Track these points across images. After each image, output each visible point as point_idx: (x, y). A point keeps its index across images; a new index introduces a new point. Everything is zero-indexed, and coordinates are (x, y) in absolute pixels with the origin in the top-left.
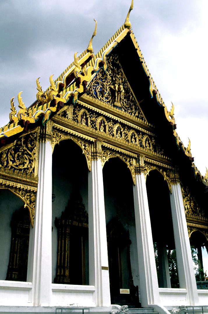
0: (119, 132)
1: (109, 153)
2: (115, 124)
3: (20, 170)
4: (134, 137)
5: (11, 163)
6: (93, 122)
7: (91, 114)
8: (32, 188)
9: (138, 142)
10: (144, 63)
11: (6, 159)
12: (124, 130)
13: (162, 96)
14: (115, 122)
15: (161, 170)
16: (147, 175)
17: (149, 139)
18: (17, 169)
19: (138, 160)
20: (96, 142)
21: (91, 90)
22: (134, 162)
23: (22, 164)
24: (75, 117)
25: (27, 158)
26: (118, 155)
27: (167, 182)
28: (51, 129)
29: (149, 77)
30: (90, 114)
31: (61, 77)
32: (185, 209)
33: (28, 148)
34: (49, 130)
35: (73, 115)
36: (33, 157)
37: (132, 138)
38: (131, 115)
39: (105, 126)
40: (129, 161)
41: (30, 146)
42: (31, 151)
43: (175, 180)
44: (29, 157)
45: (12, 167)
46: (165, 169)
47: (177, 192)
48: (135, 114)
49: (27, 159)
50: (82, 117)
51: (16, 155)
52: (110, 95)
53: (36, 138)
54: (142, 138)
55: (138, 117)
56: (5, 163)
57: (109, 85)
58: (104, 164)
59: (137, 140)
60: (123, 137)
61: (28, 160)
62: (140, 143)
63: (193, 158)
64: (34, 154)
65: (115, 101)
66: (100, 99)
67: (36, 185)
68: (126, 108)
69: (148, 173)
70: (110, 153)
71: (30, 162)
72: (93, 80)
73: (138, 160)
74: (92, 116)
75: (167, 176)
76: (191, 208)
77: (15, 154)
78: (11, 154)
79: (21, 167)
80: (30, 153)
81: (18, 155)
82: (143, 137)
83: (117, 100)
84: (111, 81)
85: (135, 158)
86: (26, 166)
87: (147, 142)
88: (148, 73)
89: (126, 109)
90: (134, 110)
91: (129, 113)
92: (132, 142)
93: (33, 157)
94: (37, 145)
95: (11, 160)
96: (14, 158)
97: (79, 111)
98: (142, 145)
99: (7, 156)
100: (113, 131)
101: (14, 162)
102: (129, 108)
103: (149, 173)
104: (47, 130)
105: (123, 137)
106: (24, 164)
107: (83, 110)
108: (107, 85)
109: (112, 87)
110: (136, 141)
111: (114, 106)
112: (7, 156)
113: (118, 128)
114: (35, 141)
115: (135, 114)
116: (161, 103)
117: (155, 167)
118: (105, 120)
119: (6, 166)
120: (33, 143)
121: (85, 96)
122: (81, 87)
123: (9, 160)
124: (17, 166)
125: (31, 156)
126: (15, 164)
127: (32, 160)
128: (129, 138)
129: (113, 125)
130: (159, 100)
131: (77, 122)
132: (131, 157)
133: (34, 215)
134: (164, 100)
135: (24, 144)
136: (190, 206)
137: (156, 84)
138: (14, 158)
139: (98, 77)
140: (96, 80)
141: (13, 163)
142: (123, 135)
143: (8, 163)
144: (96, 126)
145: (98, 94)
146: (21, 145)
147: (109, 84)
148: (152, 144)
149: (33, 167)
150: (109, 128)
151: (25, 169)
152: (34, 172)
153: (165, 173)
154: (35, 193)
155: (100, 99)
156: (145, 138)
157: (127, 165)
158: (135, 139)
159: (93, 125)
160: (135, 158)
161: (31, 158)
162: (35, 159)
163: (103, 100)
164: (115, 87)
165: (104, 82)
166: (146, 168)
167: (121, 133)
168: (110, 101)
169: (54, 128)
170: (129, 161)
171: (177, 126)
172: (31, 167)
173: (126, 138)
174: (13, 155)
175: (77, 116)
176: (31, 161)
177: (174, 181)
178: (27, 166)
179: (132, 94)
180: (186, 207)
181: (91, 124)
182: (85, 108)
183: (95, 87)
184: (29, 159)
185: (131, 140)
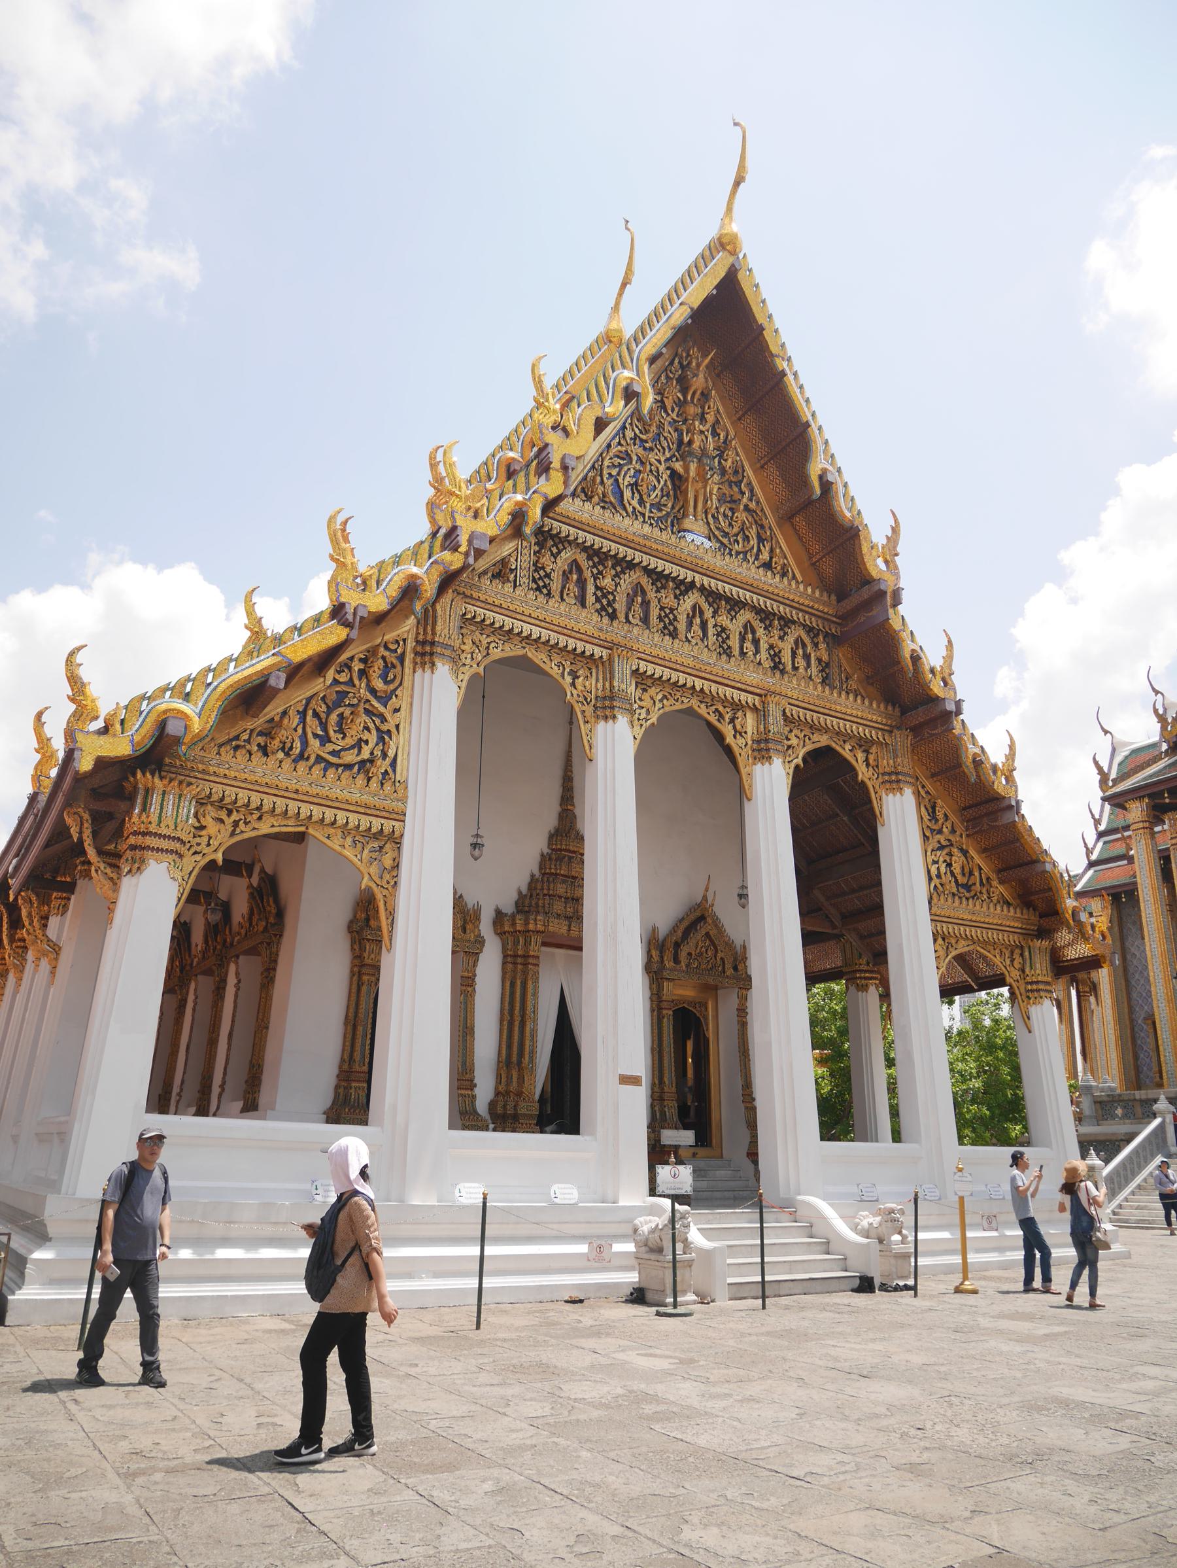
0: (698, 620)
1: (660, 696)
2: (684, 593)
3: (349, 767)
4: (750, 636)
5: (315, 744)
6: (603, 594)
7: (601, 562)
8: (388, 825)
9: (763, 655)
10: (790, 377)
11: (300, 730)
12: (715, 612)
13: (853, 491)
14: (685, 587)
15: (848, 747)
16: (797, 767)
17: (807, 640)
18: (338, 766)
19: (761, 713)
20: (610, 659)
21: (602, 482)
22: (750, 722)
23: (353, 747)
24: (540, 578)
25: (371, 726)
26: (694, 703)
27: (869, 784)
28: (456, 623)
29: (807, 425)
30: (594, 566)
31: (514, 438)
32: (930, 879)
33: (373, 691)
34: (446, 628)
35: (536, 571)
36: (390, 726)
37: (743, 639)
38: (745, 559)
39: (646, 604)
40: (732, 721)
41: (379, 684)
42: (385, 700)
43: (898, 781)
44: (377, 721)
45: (319, 759)
47: (901, 820)
48: (757, 558)
49: (369, 731)
50: (566, 576)
51: (334, 717)
52: (668, 495)
53: (401, 659)
54: (781, 638)
55: (767, 566)
56: (298, 745)
57: (667, 460)
58: (639, 732)
59: (764, 646)
60: (712, 638)
61: (374, 732)
62: (772, 657)
63: (958, 704)
64: (397, 710)
65: (685, 516)
66: (630, 509)
67: (401, 816)
68: (726, 535)
69: (799, 761)
70: (665, 697)
71: (381, 739)
72: (609, 446)
73: (761, 713)
74: (600, 573)
77: (329, 711)
78: (316, 714)
79: (350, 757)
80: (381, 709)
81: (341, 716)
82: (786, 634)
83: (691, 510)
84: (674, 447)
85: (755, 709)
86: (365, 755)
87: (800, 651)
88: (806, 415)
89: (725, 541)
90: (754, 542)
91: (738, 553)
92: (743, 654)
93: (390, 726)
94: (406, 683)
95: (316, 736)
96: (324, 726)
97: (555, 556)
98: (780, 662)
99: (303, 720)
100: (675, 619)
101: (325, 739)
102: (737, 535)
103: (804, 759)
104: (438, 628)
105: (712, 638)
106: (359, 744)
107: (567, 555)
108: (659, 461)
109: (678, 466)
110: (757, 651)
112: (303, 720)
113: (694, 607)
114: (399, 668)
115: (757, 558)
116: (848, 514)
117: (825, 737)
118: (645, 581)
119: (301, 757)
120: (391, 676)
121: (571, 507)
122: (557, 476)
123: (310, 735)
124: (333, 753)
125: (384, 719)
126: (330, 747)
127: (389, 732)
128: (734, 642)
129: (676, 597)
130: (842, 505)
131: (549, 595)
132: (737, 706)
133: (391, 915)
134: (860, 504)
135: (360, 679)
137: (833, 449)
138: (324, 726)
139: (629, 434)
140: (619, 444)
141: (322, 745)
142: (711, 631)
143: (305, 743)
144: (616, 606)
145: (627, 494)
146: (351, 683)
147: (668, 455)
148: (819, 660)
149: (391, 753)
150: (662, 609)
151: (362, 763)
152: (394, 771)
153: (861, 756)
154: (396, 840)
155: (630, 509)
158: (756, 642)
159: (605, 602)
160: (755, 709)
161: (384, 728)
162: (397, 727)
163: (644, 515)
164: (687, 469)
165: (651, 449)
166: (794, 741)
167: (704, 625)
168: (668, 514)
169: (467, 621)
170: (732, 721)
171: (904, 595)
172: (385, 755)
173: (724, 642)
174: (323, 716)
175: (548, 576)
176: (383, 737)
177: (893, 782)
178: (372, 753)
179: (749, 484)
181: (598, 600)
182: (574, 543)
183: (614, 472)
184: (378, 729)
185: (741, 648)
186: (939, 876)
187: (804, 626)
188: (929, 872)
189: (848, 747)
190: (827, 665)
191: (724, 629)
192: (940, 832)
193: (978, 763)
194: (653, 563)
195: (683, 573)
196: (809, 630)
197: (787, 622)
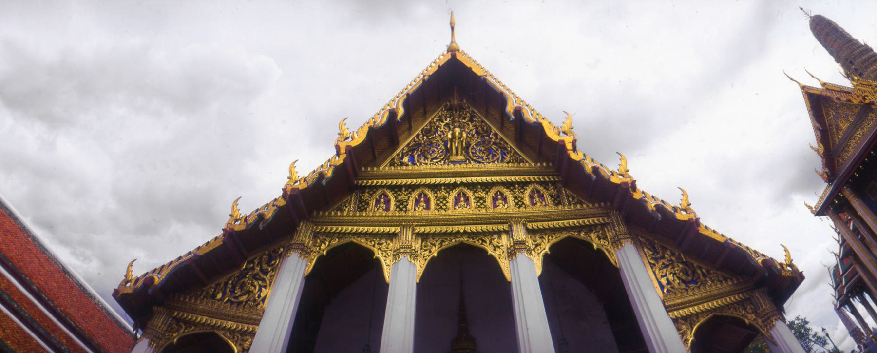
32: (662, 287)
46: (590, 228)
54: (523, 193)
63: (634, 182)
69: (547, 249)
75: (599, 239)
76: (679, 278)
103: (550, 249)
111: (454, 163)
136: (675, 274)
148: (552, 196)
156: (528, 191)
157: (485, 251)
170: (491, 243)
177: (617, 242)
180: (664, 281)
186: (669, 283)
187: (537, 183)
188: (660, 283)
189: (582, 234)
190: (558, 197)
191: (481, 199)
192: (663, 257)
193: (660, 208)
194: (428, 181)
195: (448, 180)
196: (540, 183)
197: (523, 185)
